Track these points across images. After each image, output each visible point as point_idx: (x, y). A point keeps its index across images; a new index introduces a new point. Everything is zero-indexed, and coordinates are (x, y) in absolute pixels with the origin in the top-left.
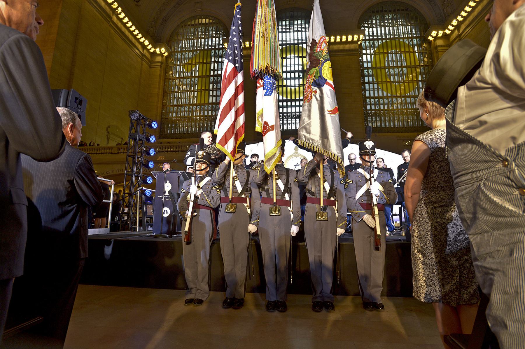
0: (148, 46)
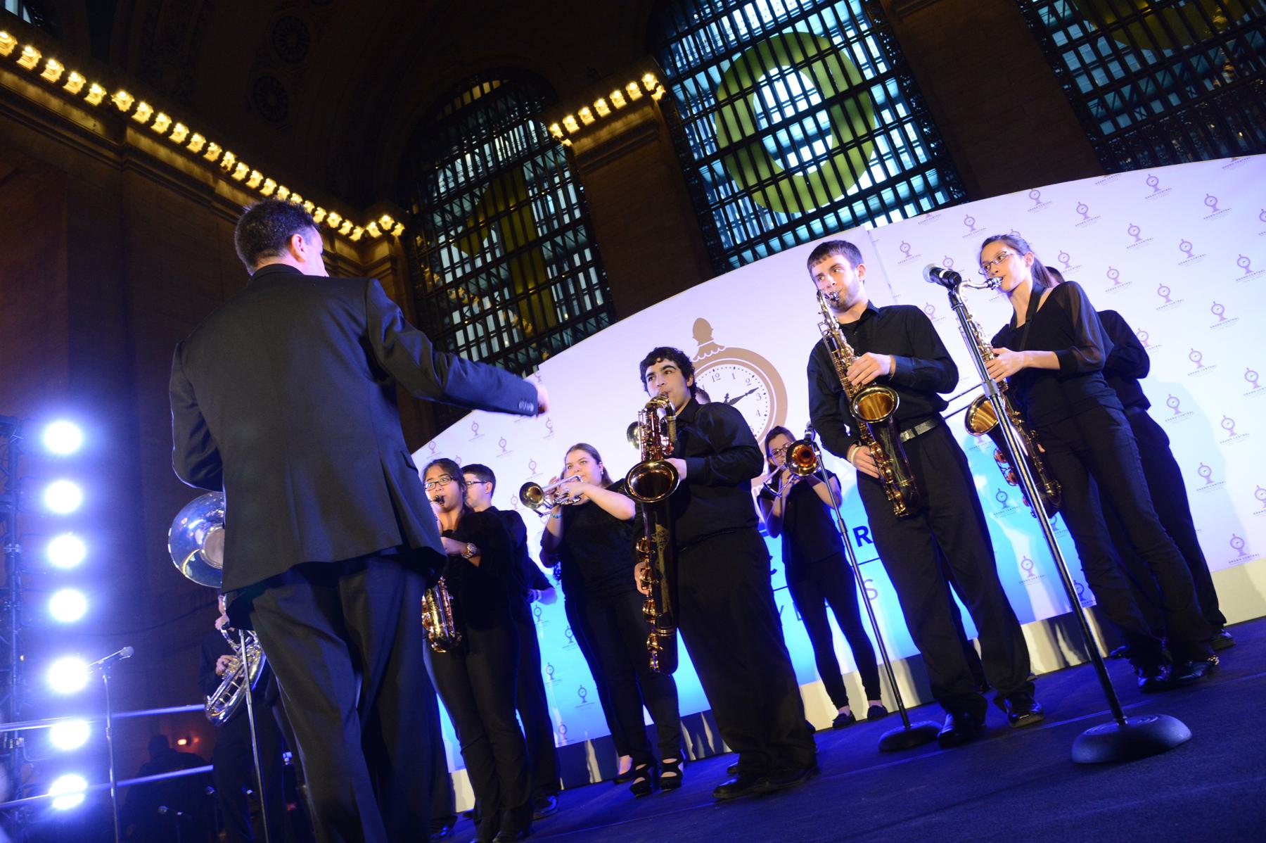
0: (340, 226)
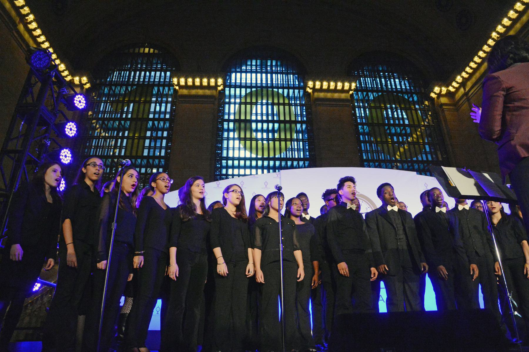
0: (63, 71)
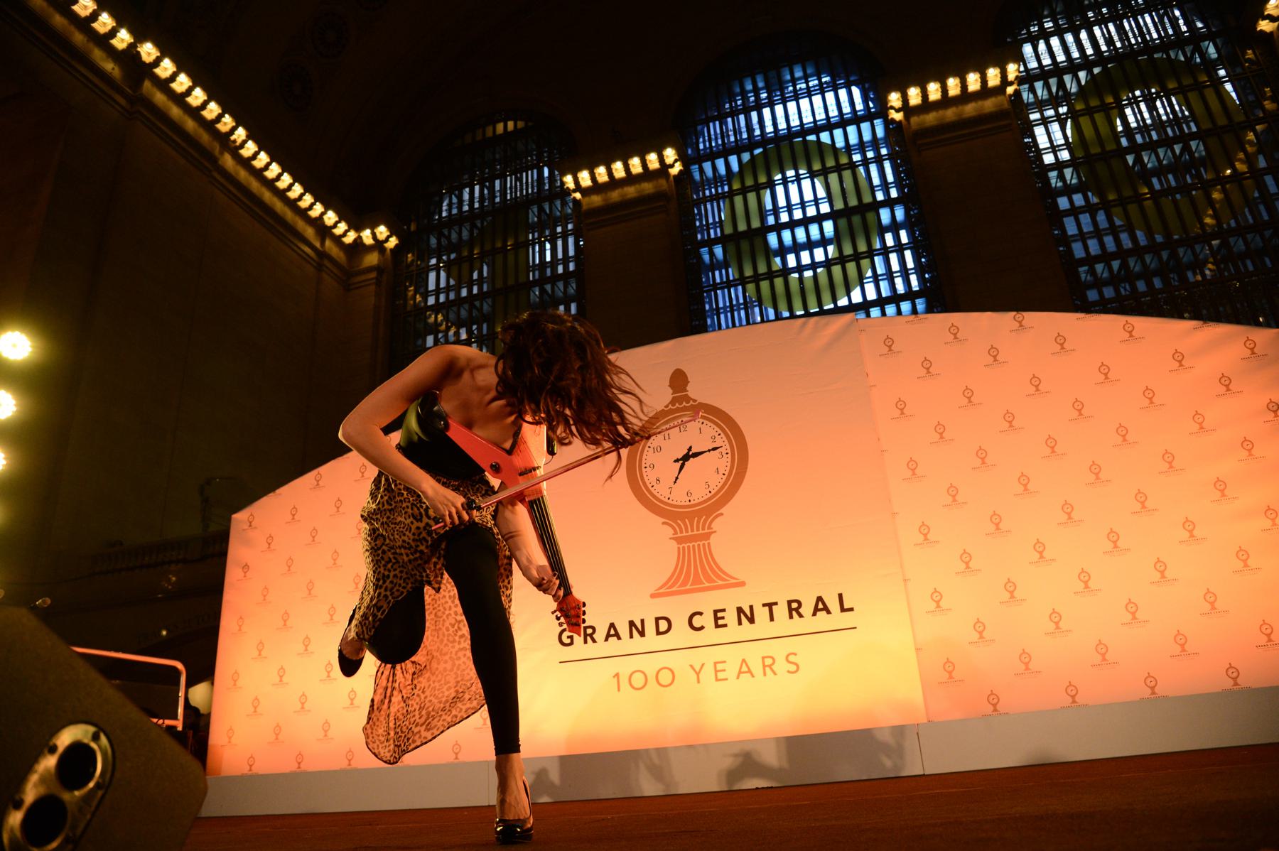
0: (335, 226)
